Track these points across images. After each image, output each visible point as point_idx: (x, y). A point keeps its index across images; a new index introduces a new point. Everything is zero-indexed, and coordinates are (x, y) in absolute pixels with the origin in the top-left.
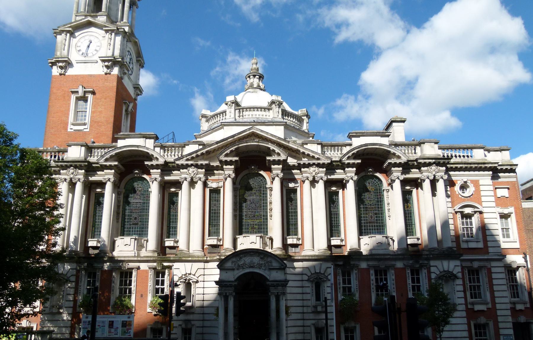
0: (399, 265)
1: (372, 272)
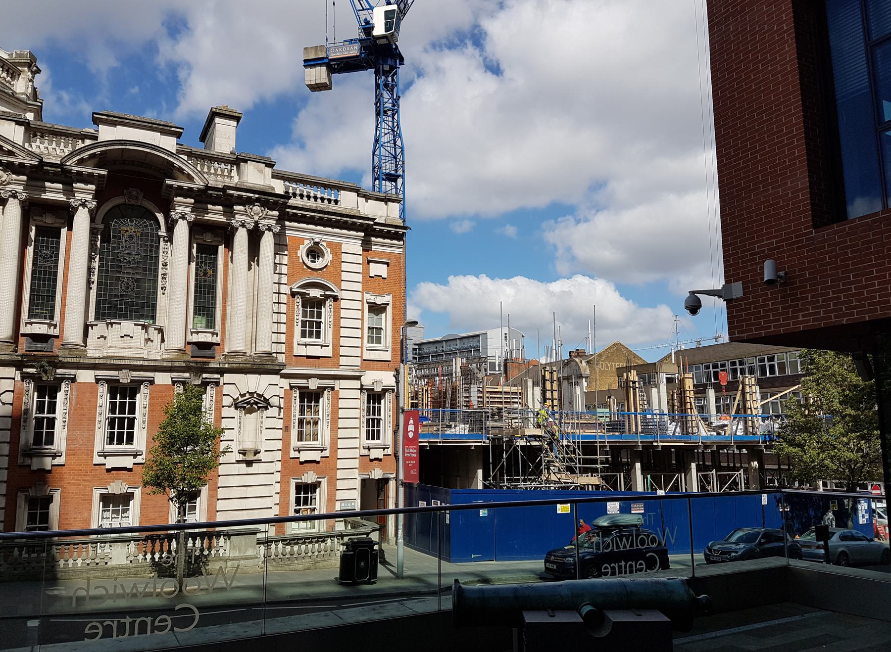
0: (163, 379)
1: (103, 389)
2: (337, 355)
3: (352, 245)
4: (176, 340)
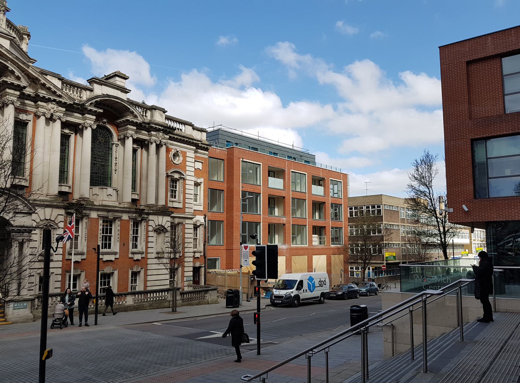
0: (125, 217)
1: (101, 222)
2: (184, 207)
3: (190, 153)
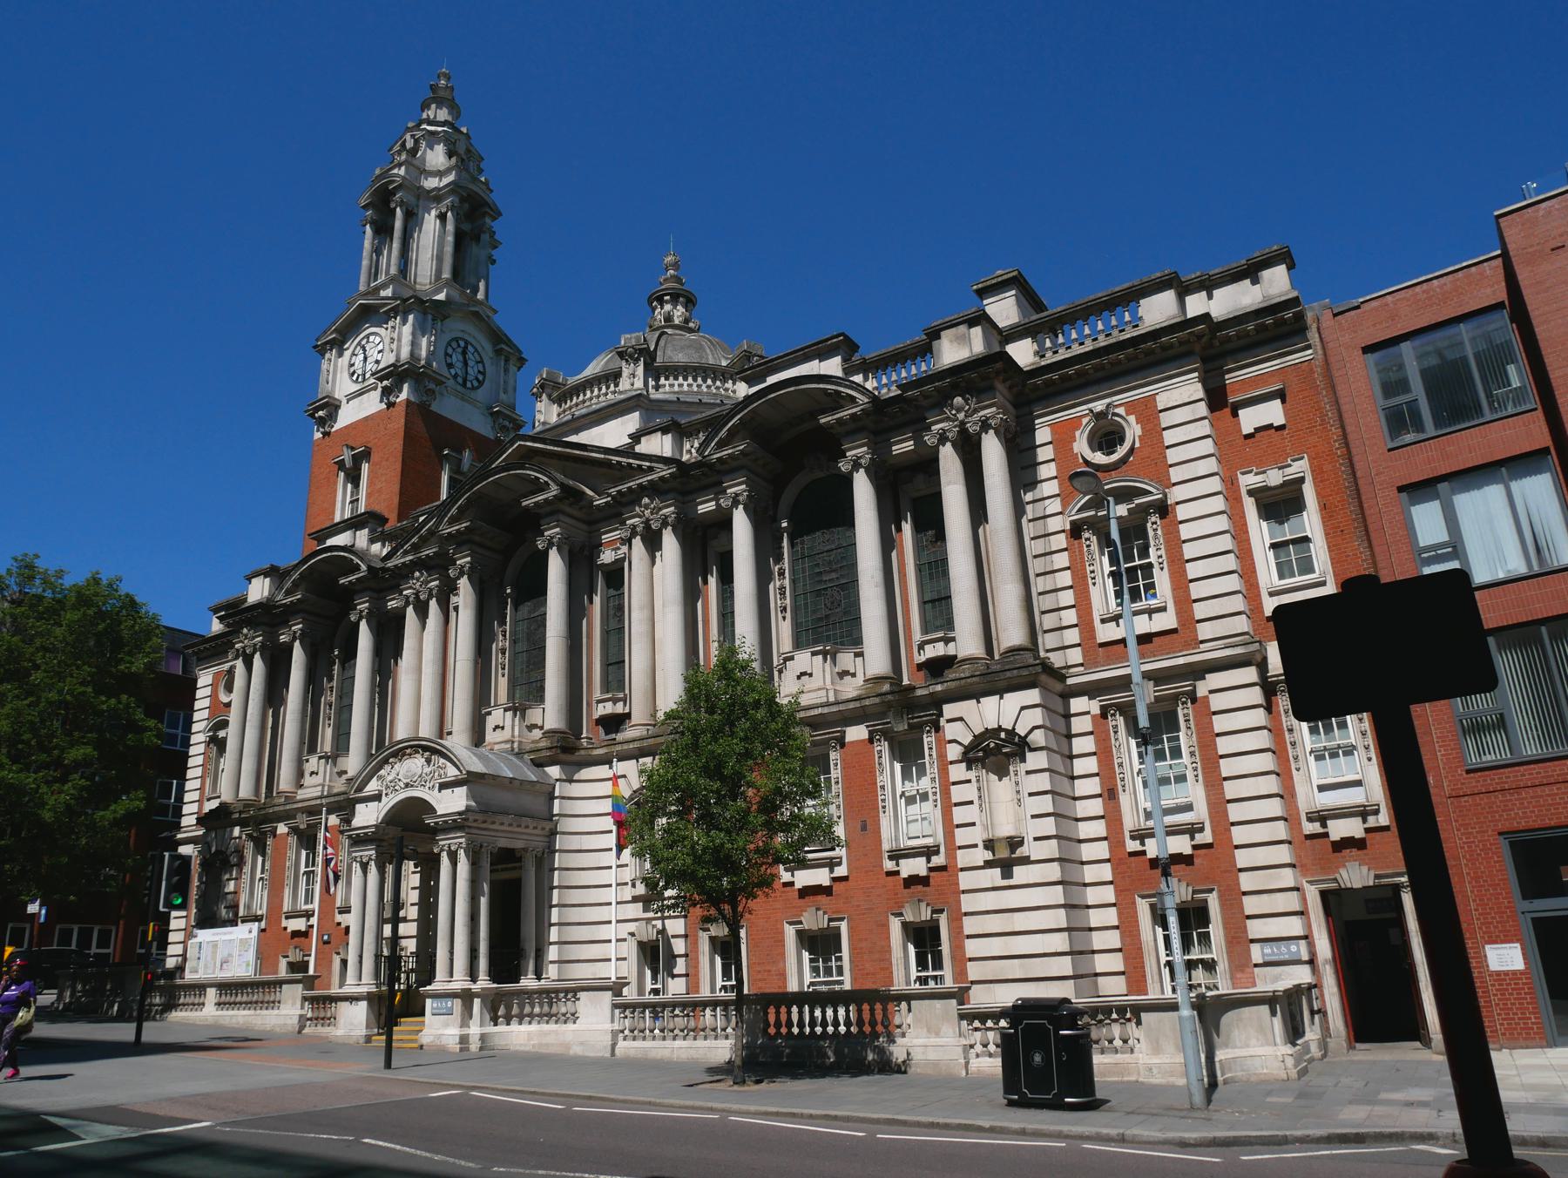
2: (1188, 620)
4: (875, 658)
